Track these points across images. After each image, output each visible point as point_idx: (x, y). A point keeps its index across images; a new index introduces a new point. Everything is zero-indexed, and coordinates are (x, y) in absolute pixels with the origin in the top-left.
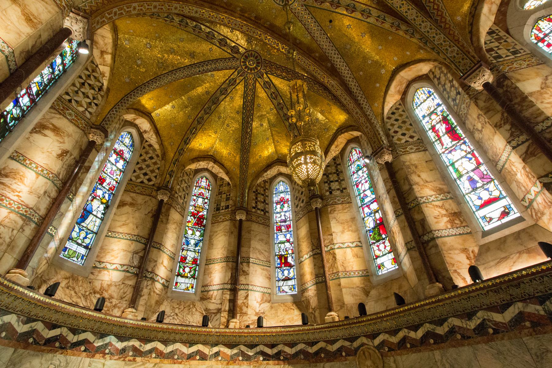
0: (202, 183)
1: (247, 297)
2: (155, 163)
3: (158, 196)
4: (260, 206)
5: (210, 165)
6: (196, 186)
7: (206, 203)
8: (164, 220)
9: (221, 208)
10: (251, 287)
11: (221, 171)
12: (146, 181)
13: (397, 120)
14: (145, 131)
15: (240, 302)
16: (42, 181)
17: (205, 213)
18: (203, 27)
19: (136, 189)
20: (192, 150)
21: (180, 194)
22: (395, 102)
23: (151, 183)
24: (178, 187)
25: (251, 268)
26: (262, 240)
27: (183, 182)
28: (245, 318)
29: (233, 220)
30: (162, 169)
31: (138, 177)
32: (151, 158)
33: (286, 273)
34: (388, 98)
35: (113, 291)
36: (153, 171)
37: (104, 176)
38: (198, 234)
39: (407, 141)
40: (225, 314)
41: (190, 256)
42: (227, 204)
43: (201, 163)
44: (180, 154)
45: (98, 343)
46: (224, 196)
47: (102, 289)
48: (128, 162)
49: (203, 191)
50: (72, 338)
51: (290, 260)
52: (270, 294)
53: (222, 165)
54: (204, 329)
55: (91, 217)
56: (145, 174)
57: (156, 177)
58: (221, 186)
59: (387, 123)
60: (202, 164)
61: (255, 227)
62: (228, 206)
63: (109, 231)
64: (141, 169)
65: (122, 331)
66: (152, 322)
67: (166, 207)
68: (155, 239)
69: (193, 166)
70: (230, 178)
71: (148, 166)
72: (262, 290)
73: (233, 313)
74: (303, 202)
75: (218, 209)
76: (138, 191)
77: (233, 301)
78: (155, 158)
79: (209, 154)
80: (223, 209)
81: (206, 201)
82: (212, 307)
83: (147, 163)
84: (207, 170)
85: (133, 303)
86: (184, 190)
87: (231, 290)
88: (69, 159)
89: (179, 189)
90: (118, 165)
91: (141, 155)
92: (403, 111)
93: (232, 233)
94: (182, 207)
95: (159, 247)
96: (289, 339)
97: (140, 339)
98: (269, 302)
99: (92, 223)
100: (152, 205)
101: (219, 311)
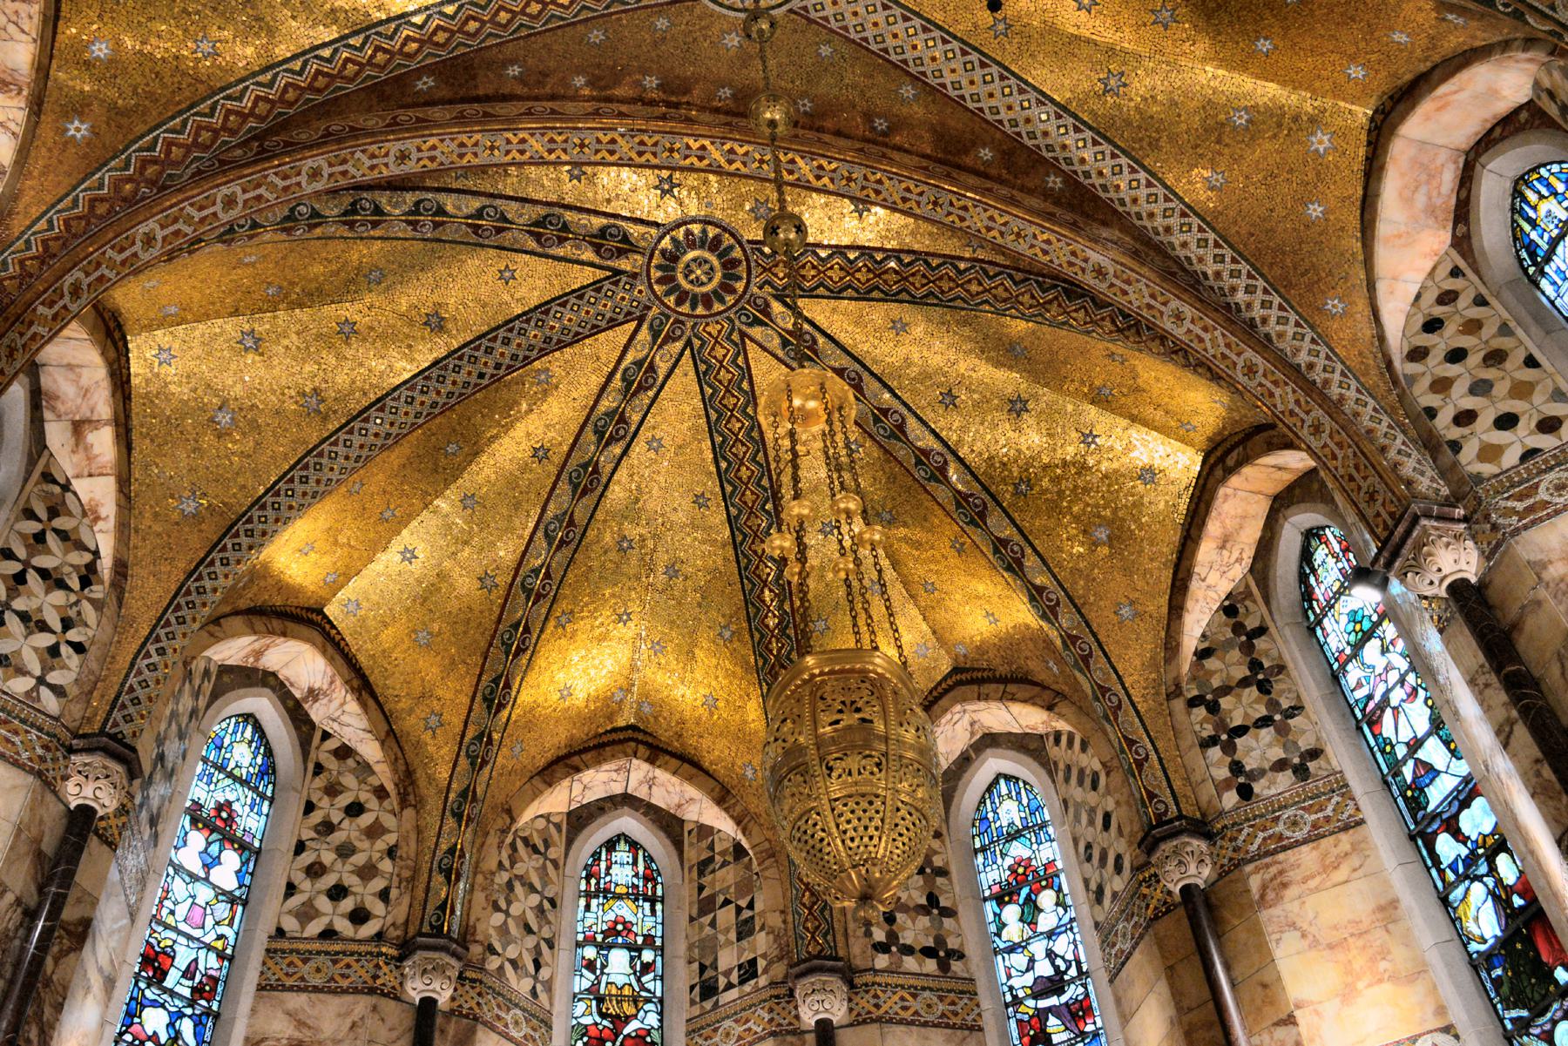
0: (615, 869)
2: (374, 831)
3: (409, 986)
5: (637, 775)
6: (589, 895)
7: (647, 968)
9: (722, 982)
11: (691, 791)
12: (343, 926)
13: (1456, 356)
14: (311, 691)
17: (652, 1020)
18: (449, 203)
19: (306, 969)
20: (532, 721)
21: (512, 952)
22: (1429, 265)
24: (498, 918)
27: (518, 889)
31: (307, 913)
32: (355, 810)
34: (1385, 258)
36: (367, 872)
39: (1529, 454)
42: (748, 956)
43: (588, 776)
44: (478, 763)
46: (726, 916)
48: (258, 852)
53: (689, 764)
56: (338, 892)
57: (384, 895)
58: (704, 866)
59: (1412, 379)
60: (598, 781)
62: (753, 962)
64: (316, 870)
67: (451, 1029)
69: (558, 800)
70: (738, 821)
74: (1118, 868)
75: (708, 990)
76: (317, 981)
78: (373, 803)
79: (621, 723)
80: (729, 986)
83: (338, 837)
84: (625, 800)
86: (528, 930)
89: (503, 930)
90: (217, 875)
91: (310, 808)
92: (1480, 301)
94: (530, 1015)
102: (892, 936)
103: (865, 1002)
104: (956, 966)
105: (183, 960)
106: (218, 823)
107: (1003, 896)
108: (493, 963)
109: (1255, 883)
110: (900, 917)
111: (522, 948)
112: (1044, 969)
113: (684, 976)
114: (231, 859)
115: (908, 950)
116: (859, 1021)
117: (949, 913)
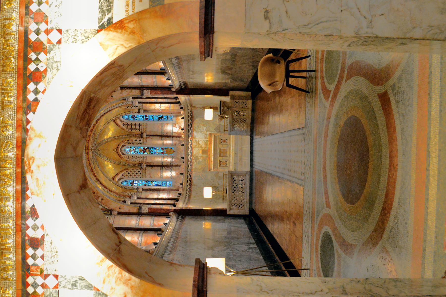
1: (175, 133)
2: (131, 171)
12: (140, 173)
16: (160, 194)
23: (140, 171)
30: (132, 169)
32: (129, 173)
38: (152, 149)
40: (180, 139)
47: (177, 174)
50: (189, 177)
51: (160, 116)
54: (185, 145)
55: (158, 184)
56: (137, 174)
61: (148, 130)
65: (187, 167)
66: (184, 160)
68: (160, 165)
69: (123, 156)
71: (133, 174)
72: (172, 127)
73: (180, 137)
75: (141, 143)
77: (176, 137)
82: (178, 142)
83: (132, 174)
85: (180, 166)
88: (151, 192)
89: (138, 160)
95: (162, 162)
97: (188, 162)
98: (175, 125)
99: (159, 183)
100: (148, 168)
101: (179, 141)
103: (144, 132)
104: (141, 124)
106: (132, 184)
107: (134, 119)
109: (145, 108)
111: (138, 159)
112: (142, 117)
113: (139, 145)
114: (135, 182)
115: (140, 128)
116: (146, 133)
117: (136, 124)
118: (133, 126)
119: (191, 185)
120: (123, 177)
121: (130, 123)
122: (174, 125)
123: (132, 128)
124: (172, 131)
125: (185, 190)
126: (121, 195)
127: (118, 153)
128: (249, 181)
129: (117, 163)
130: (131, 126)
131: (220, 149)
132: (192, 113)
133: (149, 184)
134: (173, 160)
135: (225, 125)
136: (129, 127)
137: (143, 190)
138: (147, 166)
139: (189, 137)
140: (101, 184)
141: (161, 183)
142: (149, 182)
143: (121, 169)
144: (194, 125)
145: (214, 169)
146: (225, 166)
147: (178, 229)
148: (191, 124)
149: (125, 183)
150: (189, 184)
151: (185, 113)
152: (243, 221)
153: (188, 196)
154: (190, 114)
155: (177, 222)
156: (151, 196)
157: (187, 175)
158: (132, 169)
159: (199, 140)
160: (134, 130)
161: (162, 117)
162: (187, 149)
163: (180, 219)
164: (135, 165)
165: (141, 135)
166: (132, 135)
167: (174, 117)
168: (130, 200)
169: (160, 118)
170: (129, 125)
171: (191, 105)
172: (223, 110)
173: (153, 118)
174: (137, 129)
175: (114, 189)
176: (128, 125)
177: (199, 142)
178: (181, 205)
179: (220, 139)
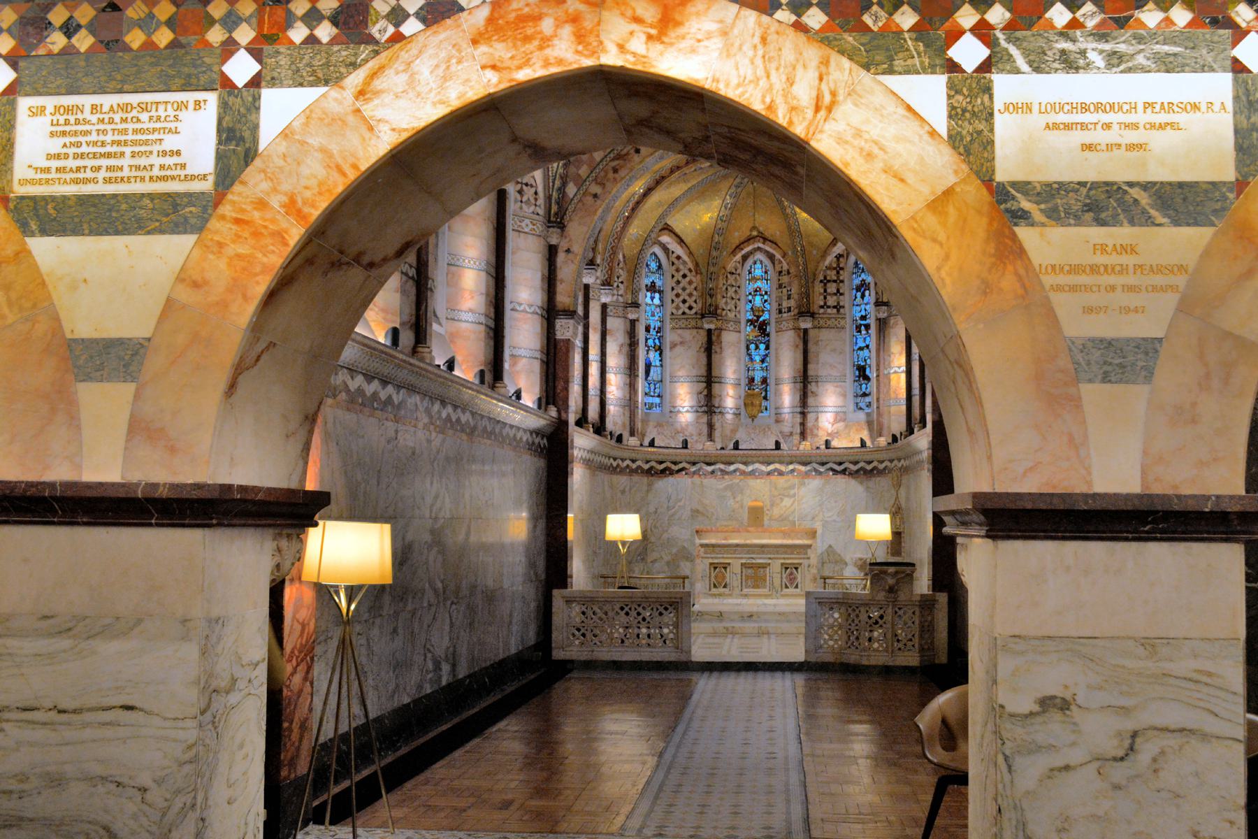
2: (690, 283)
4: (831, 301)
7: (766, 301)
8: (718, 350)
10: (821, 409)
12: (687, 311)
15: (810, 424)
16: (619, 376)
23: (694, 311)
25: (821, 388)
26: (834, 350)
28: (816, 439)
29: (797, 329)
32: (684, 276)
33: (864, 386)
35: (691, 429)
36: (690, 295)
37: (648, 322)
38: (762, 346)
40: (797, 437)
41: (758, 376)
45: (693, 469)
47: (682, 431)
49: (759, 284)
50: (675, 468)
51: (868, 372)
52: (845, 412)
54: (776, 452)
55: (652, 370)
56: (684, 301)
57: (695, 302)
61: (825, 335)
63: (671, 377)
65: (708, 460)
66: (729, 451)
68: (713, 374)
69: (738, 257)
72: (835, 409)
75: (780, 312)
77: (803, 424)
78: (688, 274)
81: (766, 297)
82: (787, 430)
83: (681, 285)
85: (710, 437)
87: (801, 413)
88: (626, 349)
93: (797, 346)
96: (852, 458)
98: (844, 420)
101: (791, 434)
102: (825, 303)
103: (816, 323)
105: (652, 327)
106: (652, 288)
107: (858, 289)
108: (724, 313)
109: (892, 322)
110: (828, 297)
113: (775, 306)
114: (657, 295)
115: (829, 307)
116: (815, 327)
117: (842, 294)
118: (834, 285)
119: (649, 472)
120: (673, 258)
121: (844, 275)
122: (840, 417)
123: (829, 285)
124: (821, 409)
125: (634, 456)
126: (614, 253)
127: (749, 240)
128: (659, 659)
129: (716, 238)
130: (835, 281)
131: (764, 566)
132: (881, 472)
133: (650, 342)
134: (729, 417)
135: (845, 581)
136: (832, 275)
137: (633, 323)
138: (709, 332)
139: (805, 464)
140: (649, 191)
141: (655, 378)
142: (657, 341)
143: (699, 252)
144: (841, 479)
145: (702, 545)
146: (713, 579)
147: (501, 433)
148: (845, 469)
149: (653, 266)
150: (652, 468)
151: (879, 450)
152: (531, 638)
153: (615, 464)
154: (875, 468)
155: (525, 431)
156: (612, 348)
157: (683, 458)
158: (700, 287)
159: (794, 495)
160: (822, 291)
161: (867, 378)
162: (766, 459)
163: (537, 440)
164: (711, 296)
165: (805, 311)
166: (807, 288)
167: (868, 415)
168: (598, 282)
169: (862, 373)
170: (838, 273)
171: (905, 470)
172: (885, 572)
173: (861, 349)
174: (825, 298)
175: (635, 230)
176: (839, 269)
177: (788, 496)
178: (582, 442)
179: (801, 564)
